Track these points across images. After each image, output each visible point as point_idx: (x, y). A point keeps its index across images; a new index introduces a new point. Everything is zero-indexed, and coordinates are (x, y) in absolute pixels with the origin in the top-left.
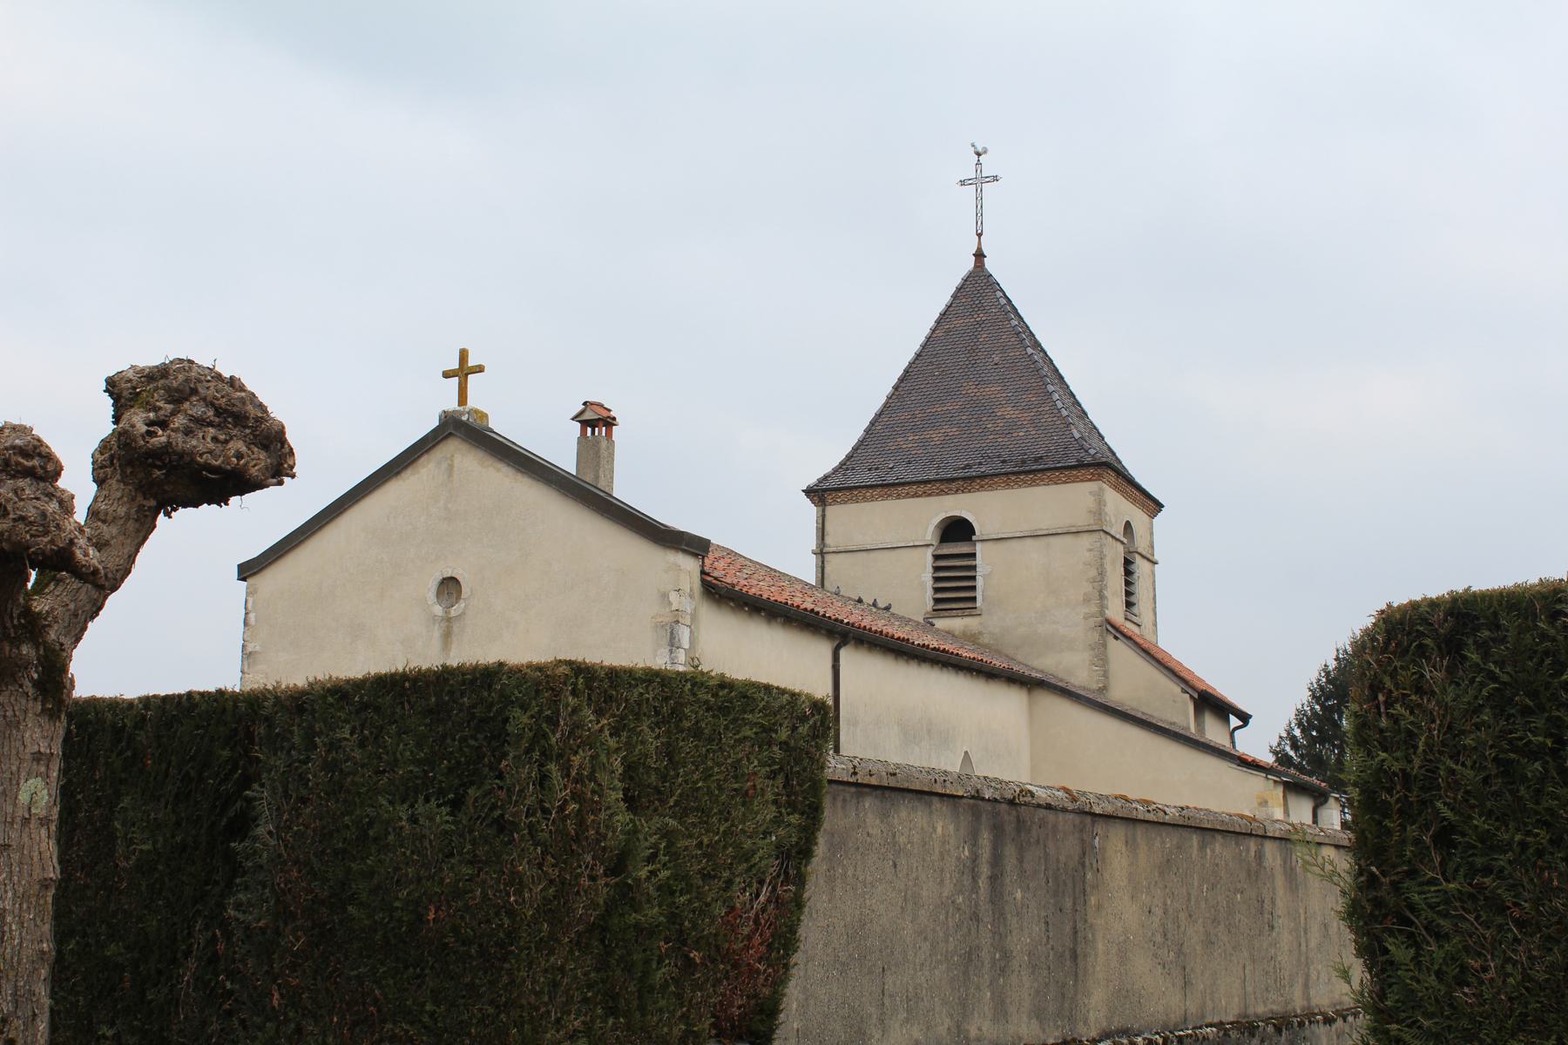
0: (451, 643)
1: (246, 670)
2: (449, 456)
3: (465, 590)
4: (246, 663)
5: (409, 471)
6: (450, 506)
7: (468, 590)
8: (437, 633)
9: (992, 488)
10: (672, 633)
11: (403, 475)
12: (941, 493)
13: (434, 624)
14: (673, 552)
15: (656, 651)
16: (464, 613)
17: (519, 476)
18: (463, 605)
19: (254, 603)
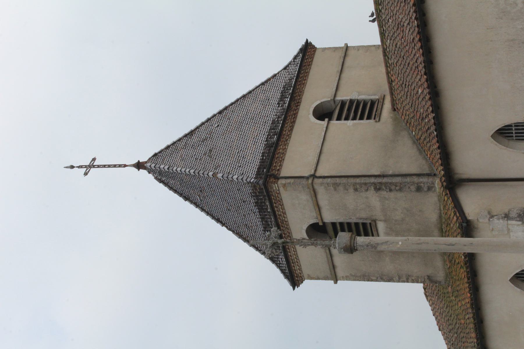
9: (302, 92)
12: (295, 115)
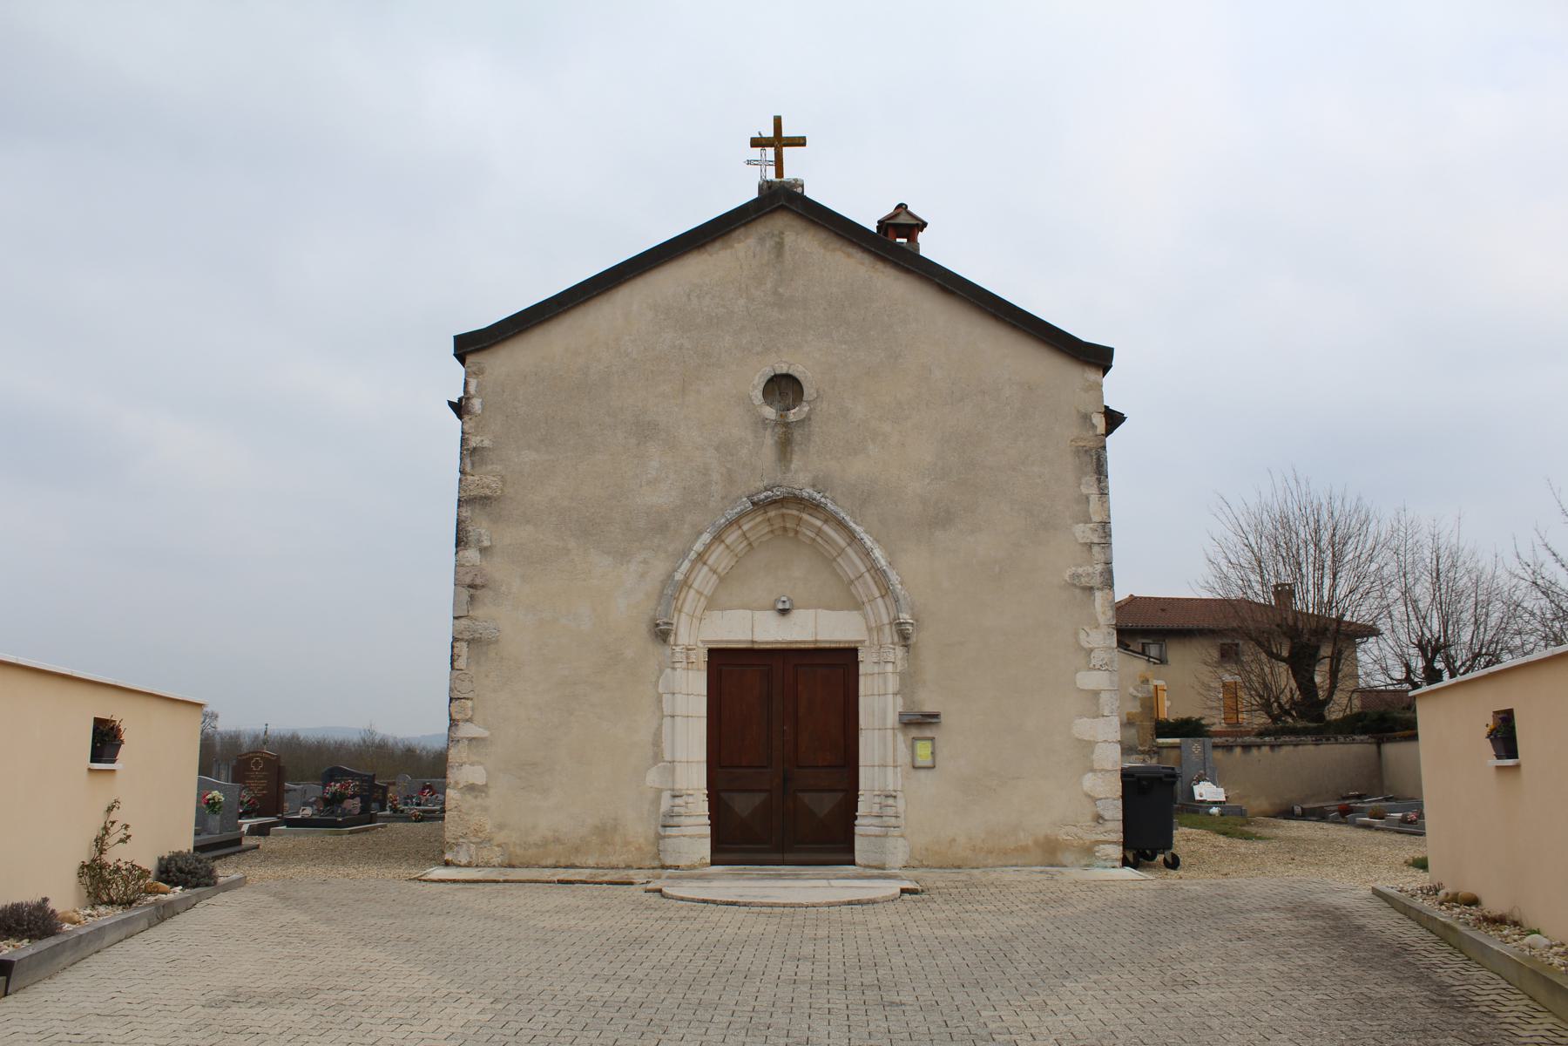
0: (791, 454)
1: (468, 469)
2: (776, 232)
3: (809, 391)
4: (468, 461)
5: (718, 245)
6: (781, 290)
7: (812, 391)
8: (769, 440)
10: (1098, 459)
11: (708, 248)
13: (766, 429)
14: (1093, 370)
15: (1080, 479)
16: (808, 418)
17: (880, 266)
18: (806, 409)
19: (478, 382)
